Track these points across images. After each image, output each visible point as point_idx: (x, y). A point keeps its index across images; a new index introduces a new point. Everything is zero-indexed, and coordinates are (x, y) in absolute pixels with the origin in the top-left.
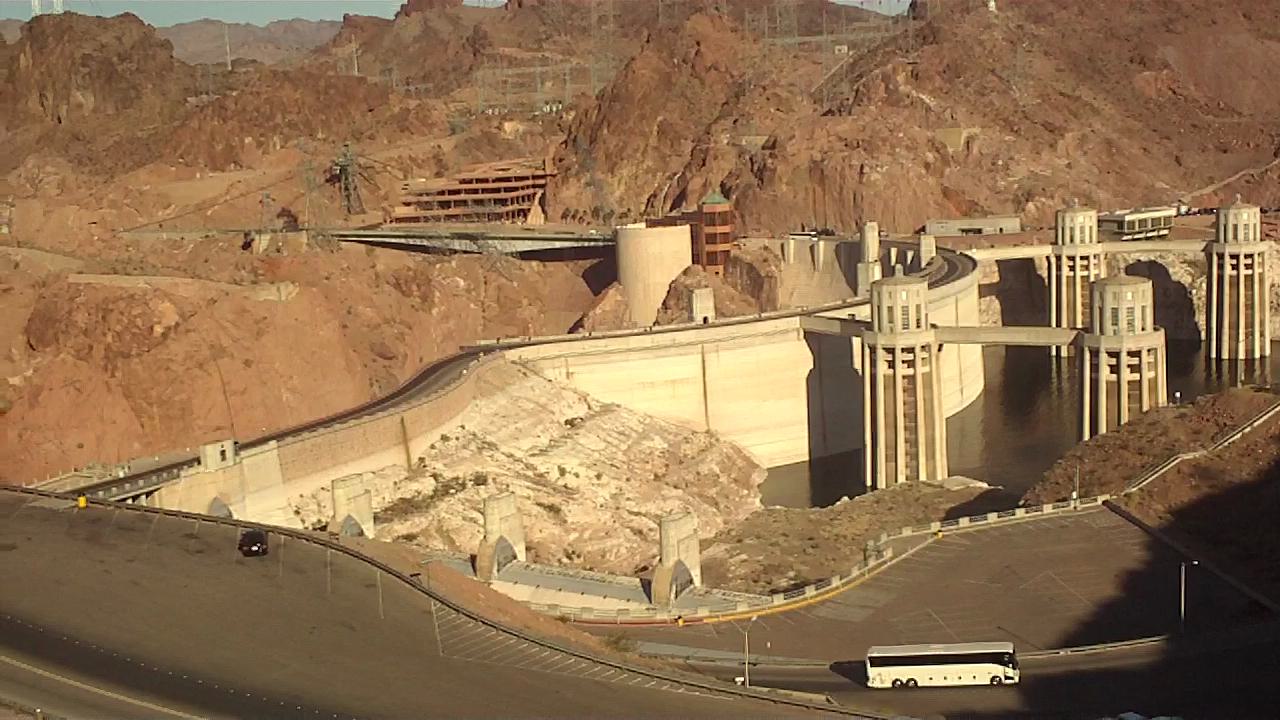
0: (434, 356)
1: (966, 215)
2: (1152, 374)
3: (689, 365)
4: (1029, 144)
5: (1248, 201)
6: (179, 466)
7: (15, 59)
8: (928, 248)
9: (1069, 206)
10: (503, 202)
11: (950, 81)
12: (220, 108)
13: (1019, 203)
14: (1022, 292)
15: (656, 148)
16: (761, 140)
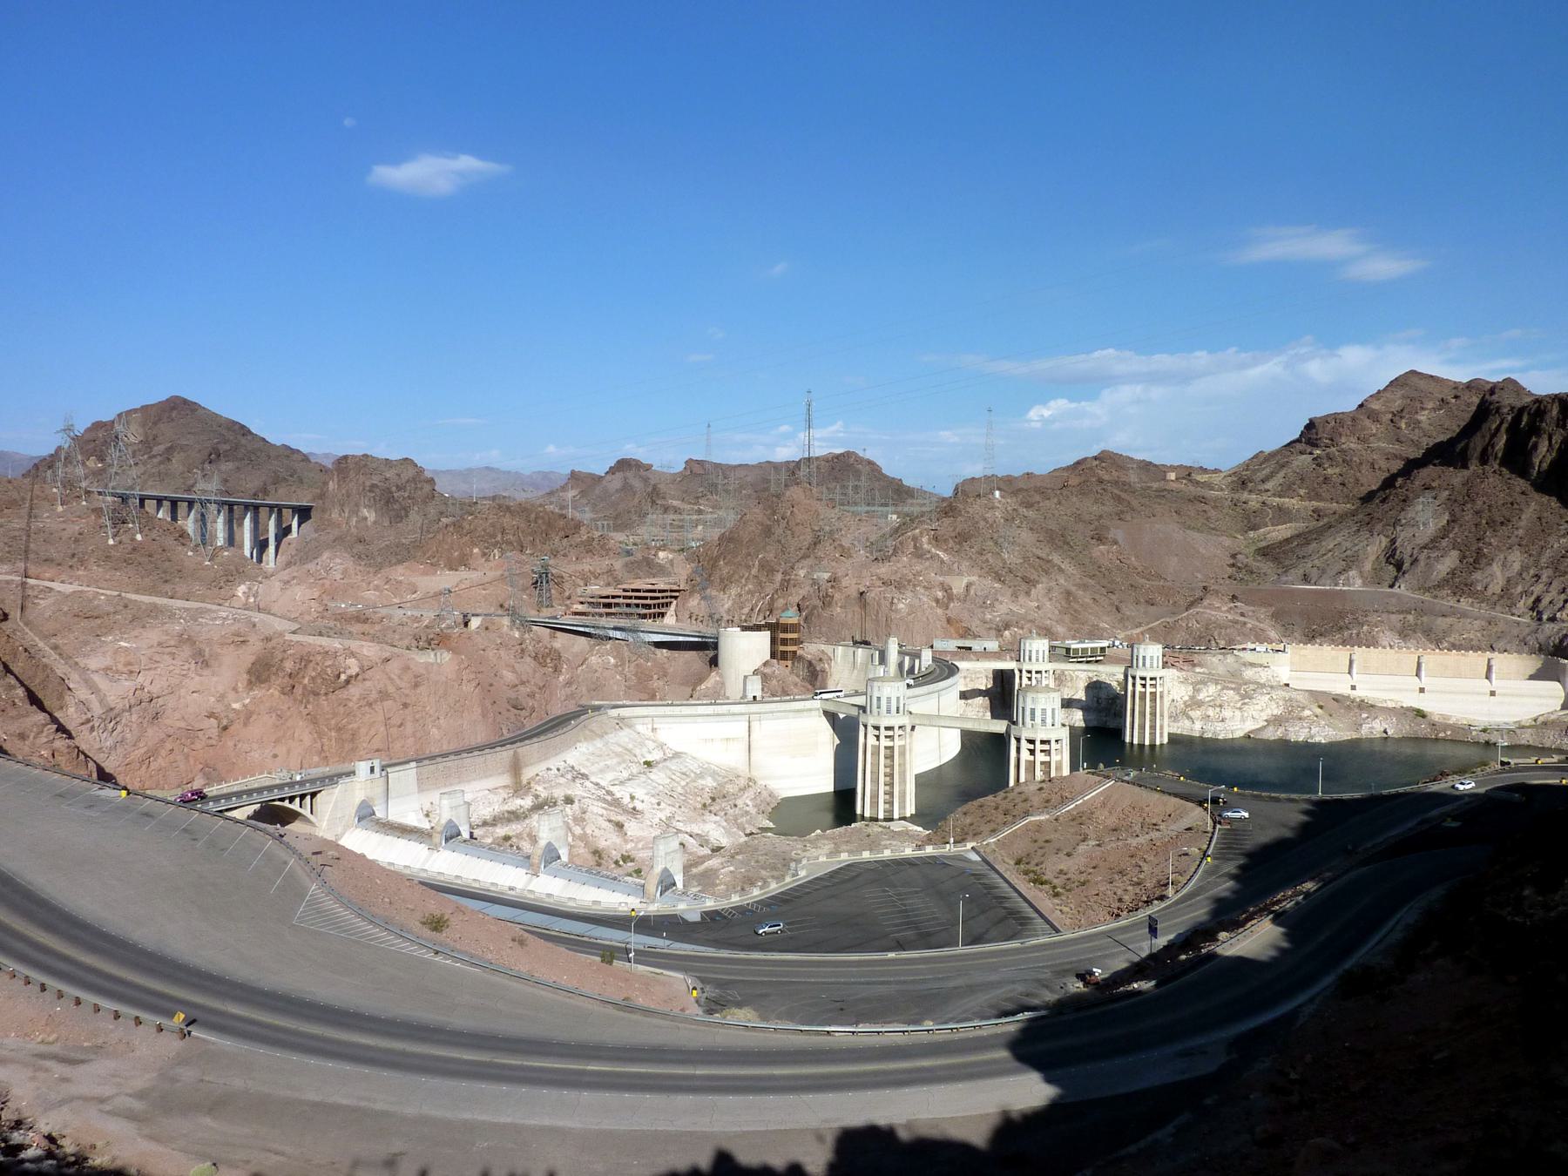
0: (557, 710)
1: (962, 637)
3: (738, 728)
5: (1155, 639)
6: (340, 776)
7: (326, 483)
8: (927, 657)
9: (1029, 635)
10: (648, 606)
11: (960, 543)
16: (826, 576)
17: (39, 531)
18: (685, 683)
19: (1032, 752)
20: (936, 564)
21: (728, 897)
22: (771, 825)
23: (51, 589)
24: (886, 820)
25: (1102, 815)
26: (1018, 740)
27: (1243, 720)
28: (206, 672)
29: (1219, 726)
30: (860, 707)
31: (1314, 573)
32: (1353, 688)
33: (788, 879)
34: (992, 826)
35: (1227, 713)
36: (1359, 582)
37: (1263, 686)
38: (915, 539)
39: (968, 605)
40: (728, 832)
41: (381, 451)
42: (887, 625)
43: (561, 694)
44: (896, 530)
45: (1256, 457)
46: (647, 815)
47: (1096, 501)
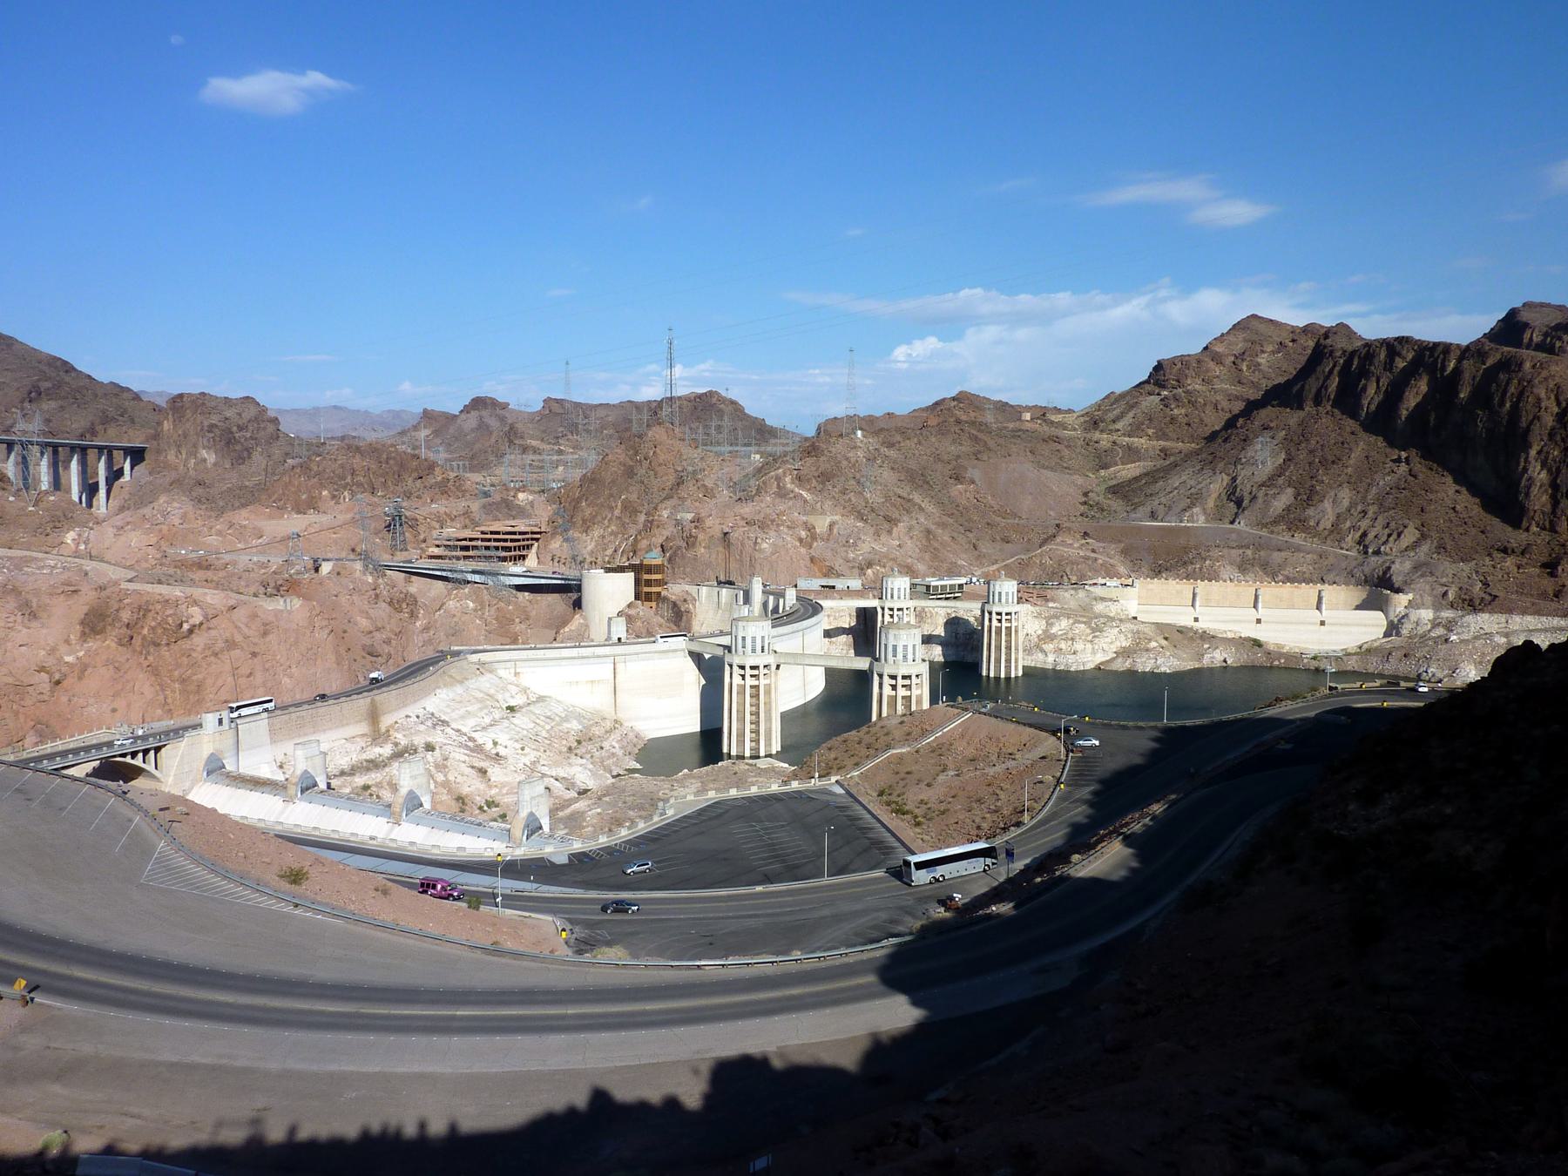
0: (415, 656)
1: (826, 576)
4: (872, 530)
5: (1010, 576)
6: (186, 728)
7: (159, 423)
8: (791, 595)
10: (508, 549)
11: (823, 483)
12: (305, 468)
13: (862, 570)
14: (865, 632)
16: (690, 516)
19: (894, 687)
20: (799, 503)
21: (594, 837)
22: (638, 766)
24: (752, 757)
25: (960, 746)
26: (881, 676)
27: (1094, 652)
28: (34, 624)
29: (1071, 659)
30: (725, 647)
31: (1161, 511)
32: (1196, 620)
33: (656, 819)
34: (855, 759)
35: (1079, 646)
36: (1202, 518)
37: (1112, 619)
38: (778, 479)
39: (831, 544)
40: (594, 774)
42: (751, 565)
43: (418, 640)
44: (759, 470)
45: (1107, 397)
46: (511, 760)
47: (954, 441)
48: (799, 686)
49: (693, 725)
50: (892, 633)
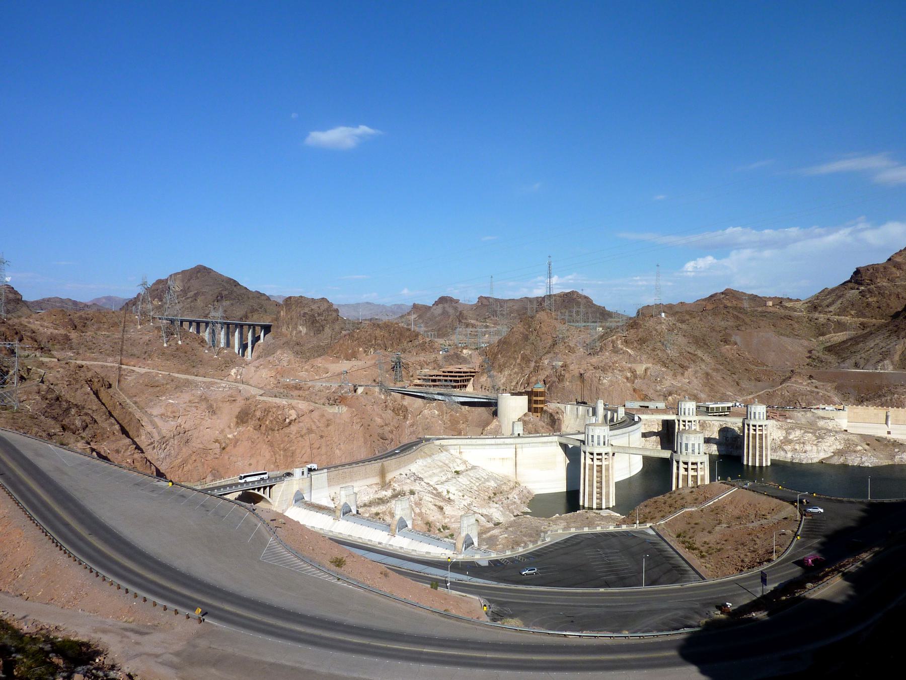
0: (405, 441)
1: (643, 400)
2: (702, 473)
4: (672, 373)
5: (762, 402)
7: (279, 312)
8: (621, 412)
12: (351, 335)
14: (667, 434)
15: (519, 364)
16: (560, 364)
17: (129, 339)
18: (479, 426)
19: (686, 470)
21: (503, 551)
22: (529, 511)
23: (134, 371)
24: (597, 509)
26: (678, 462)
27: (818, 452)
28: (215, 417)
29: (803, 456)
30: (581, 441)
31: (862, 362)
33: (539, 543)
34: (662, 514)
35: (808, 447)
36: (891, 367)
37: (830, 431)
38: (613, 342)
39: (646, 381)
40: (503, 514)
41: (309, 295)
44: (602, 337)
46: (457, 503)
47: (723, 319)
48: (626, 467)
49: (560, 486)
50: (684, 436)
